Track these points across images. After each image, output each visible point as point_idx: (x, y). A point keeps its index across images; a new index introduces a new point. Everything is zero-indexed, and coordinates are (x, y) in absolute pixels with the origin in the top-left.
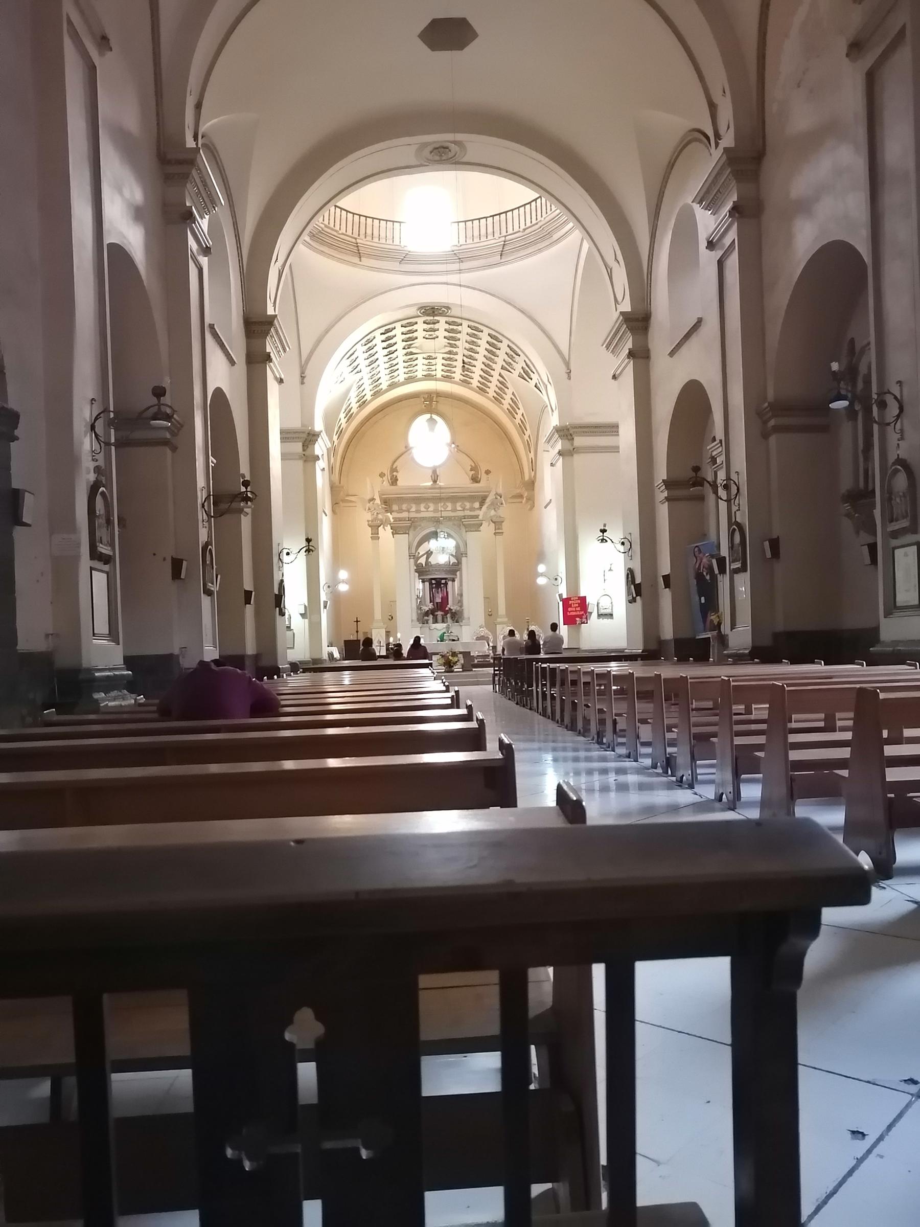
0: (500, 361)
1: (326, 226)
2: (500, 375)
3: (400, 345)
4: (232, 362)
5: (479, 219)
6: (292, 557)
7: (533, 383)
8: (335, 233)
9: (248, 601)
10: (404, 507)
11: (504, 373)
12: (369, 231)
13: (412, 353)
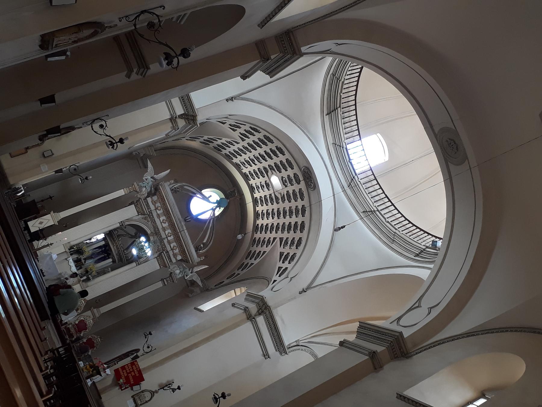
0: (285, 235)
1: (343, 82)
2: (275, 239)
3: (271, 162)
4: (263, 24)
5: (381, 188)
6: (100, 131)
7: (280, 264)
9: (43, 101)
10: (158, 204)
11: (278, 240)
12: (346, 115)
13: (267, 172)
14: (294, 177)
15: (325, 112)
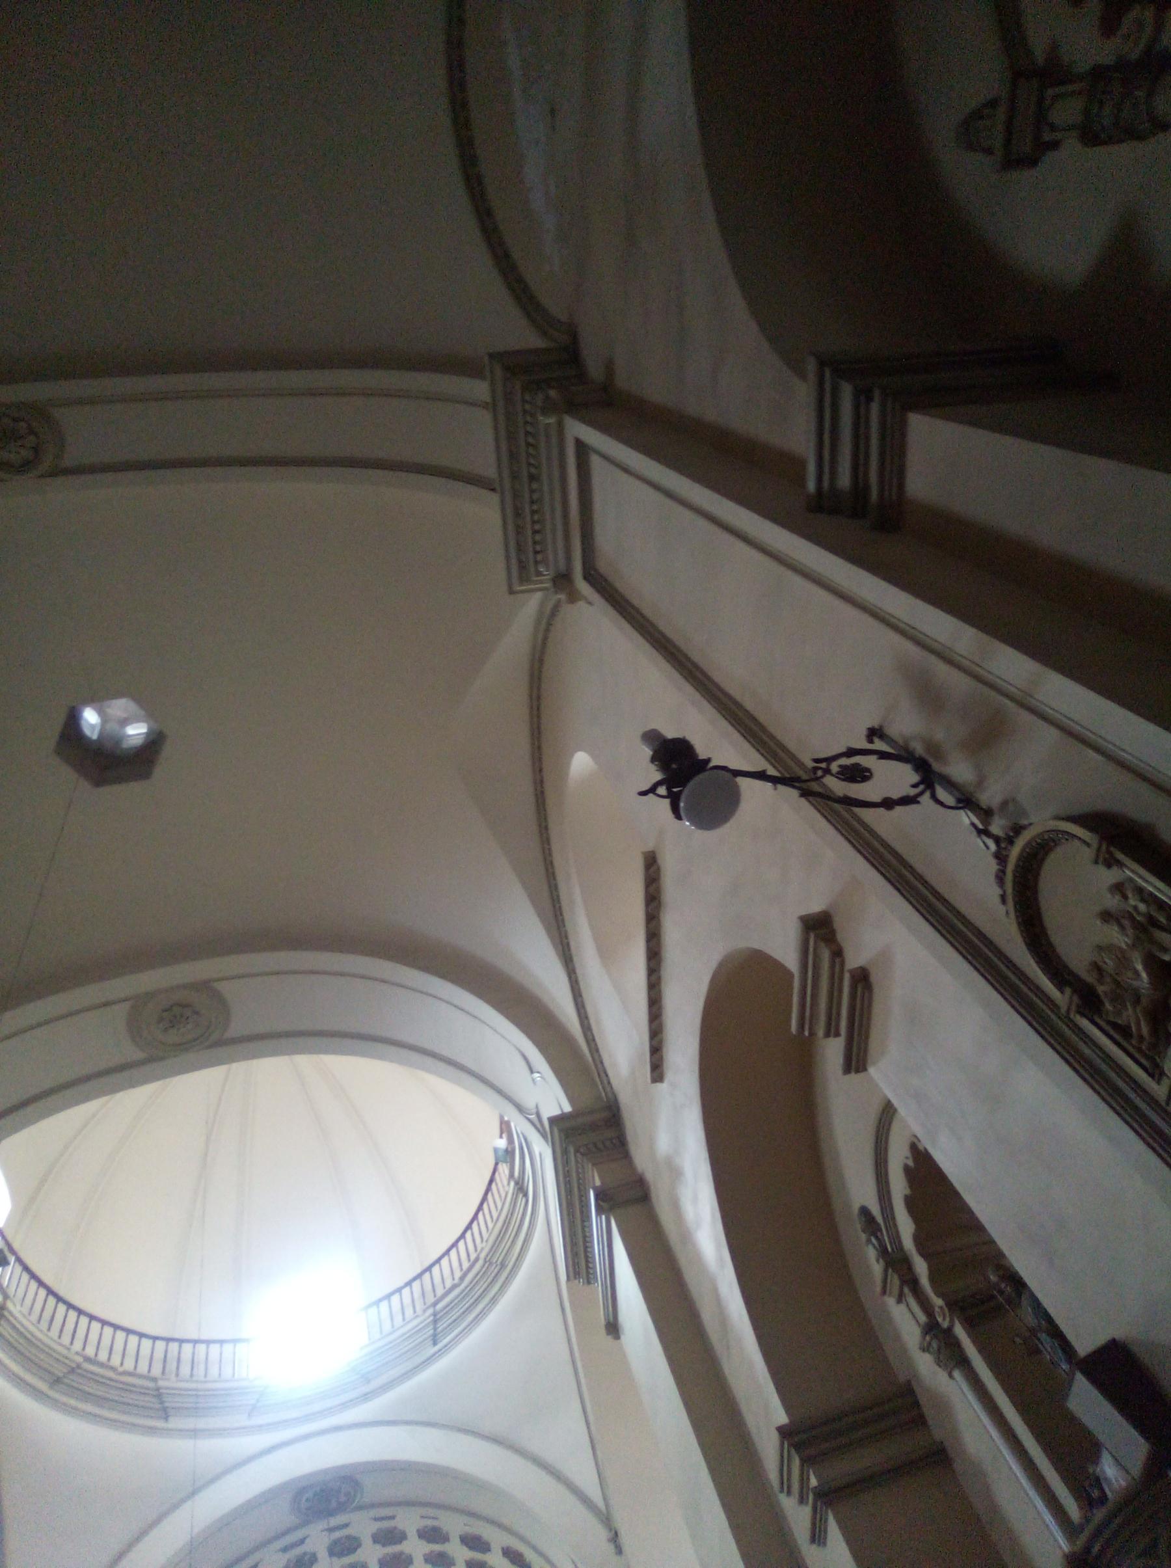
1: (87, 1359)
8: (111, 1374)
14: (341, 1554)
15: (160, 1424)
